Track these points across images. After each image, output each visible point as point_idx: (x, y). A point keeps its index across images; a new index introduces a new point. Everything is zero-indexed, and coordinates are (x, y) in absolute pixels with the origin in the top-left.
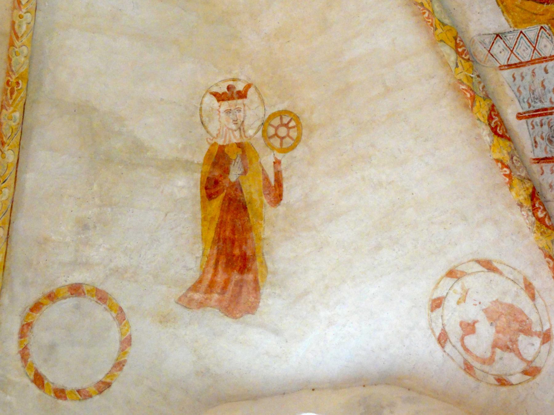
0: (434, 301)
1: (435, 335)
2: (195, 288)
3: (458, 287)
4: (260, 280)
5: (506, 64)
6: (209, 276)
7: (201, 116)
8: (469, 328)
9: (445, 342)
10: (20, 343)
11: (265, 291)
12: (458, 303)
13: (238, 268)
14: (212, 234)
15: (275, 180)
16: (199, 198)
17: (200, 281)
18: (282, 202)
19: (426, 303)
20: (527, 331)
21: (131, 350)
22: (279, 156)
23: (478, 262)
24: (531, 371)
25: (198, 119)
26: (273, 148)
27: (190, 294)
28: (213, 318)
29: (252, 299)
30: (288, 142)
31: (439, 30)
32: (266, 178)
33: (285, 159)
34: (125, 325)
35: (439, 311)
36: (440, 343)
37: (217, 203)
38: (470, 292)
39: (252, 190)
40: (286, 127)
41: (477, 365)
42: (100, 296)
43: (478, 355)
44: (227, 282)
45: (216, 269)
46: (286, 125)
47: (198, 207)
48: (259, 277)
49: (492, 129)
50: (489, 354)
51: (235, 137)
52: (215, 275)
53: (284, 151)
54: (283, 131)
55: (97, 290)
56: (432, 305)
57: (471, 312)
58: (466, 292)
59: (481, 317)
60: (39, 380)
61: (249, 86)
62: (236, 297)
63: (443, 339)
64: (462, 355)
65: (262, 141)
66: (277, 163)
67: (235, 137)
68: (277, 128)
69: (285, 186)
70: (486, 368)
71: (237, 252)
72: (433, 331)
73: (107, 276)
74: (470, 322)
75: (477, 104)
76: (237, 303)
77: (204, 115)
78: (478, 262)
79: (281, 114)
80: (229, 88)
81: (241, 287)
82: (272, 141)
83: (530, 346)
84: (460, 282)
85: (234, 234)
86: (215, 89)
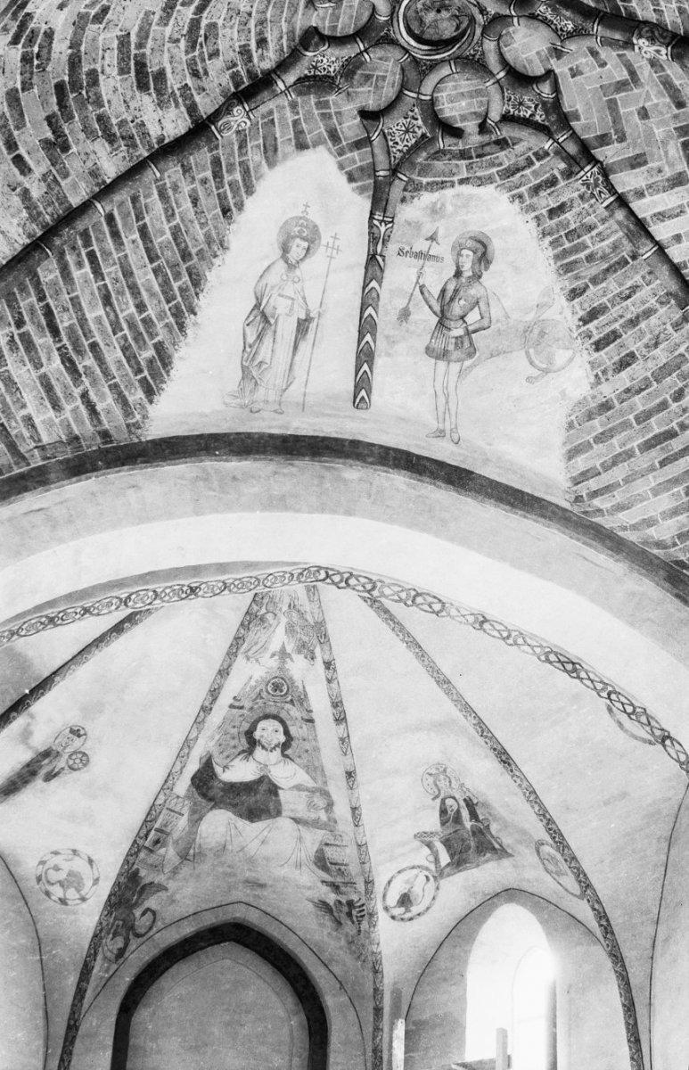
8: (57, 868)
24: (63, 901)
32: (53, 770)
37: (27, 769)
54: (78, 761)
57: (66, 867)
59: (66, 871)
61: (85, 734)
63: (42, 863)
66: (63, 769)
79: (84, 754)
80: (78, 730)
83: (72, 894)
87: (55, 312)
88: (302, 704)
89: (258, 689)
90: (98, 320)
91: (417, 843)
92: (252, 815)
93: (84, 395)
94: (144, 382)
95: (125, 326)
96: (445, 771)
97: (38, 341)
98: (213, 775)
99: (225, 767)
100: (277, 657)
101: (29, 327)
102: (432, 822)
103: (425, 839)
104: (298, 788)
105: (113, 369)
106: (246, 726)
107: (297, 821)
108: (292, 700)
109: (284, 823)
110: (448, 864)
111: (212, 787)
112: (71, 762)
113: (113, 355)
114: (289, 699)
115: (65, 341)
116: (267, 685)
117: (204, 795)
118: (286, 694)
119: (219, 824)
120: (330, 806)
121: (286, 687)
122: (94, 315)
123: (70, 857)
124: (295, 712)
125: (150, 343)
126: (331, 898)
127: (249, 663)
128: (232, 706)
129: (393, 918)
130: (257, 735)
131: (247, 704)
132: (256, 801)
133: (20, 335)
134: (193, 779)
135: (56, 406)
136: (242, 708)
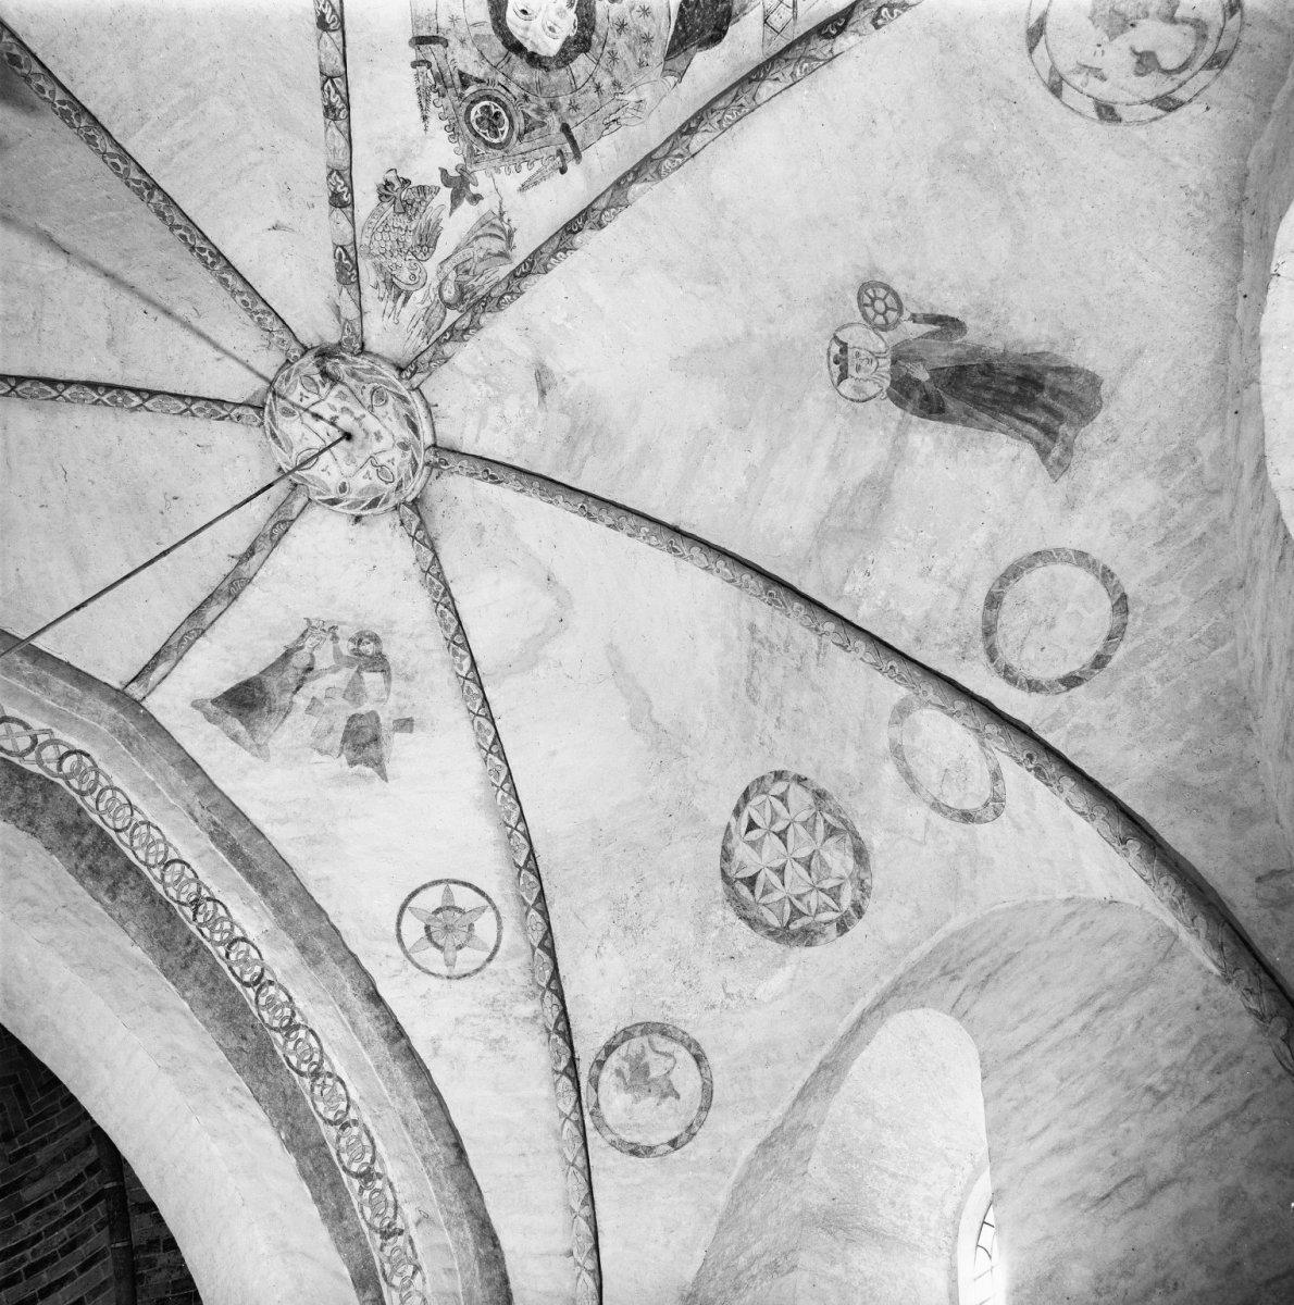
0: (1100, 115)
1: (1161, 117)
2: (1044, 453)
3: (1078, 80)
4: (1057, 365)
5: (791, 10)
6: (1034, 431)
7: (858, 401)
8: (1145, 62)
9: (1174, 101)
10: (1021, 687)
11: (1073, 359)
12: (1103, 79)
13: (1034, 391)
14: (985, 417)
15: (934, 324)
16: (940, 424)
17: (1037, 445)
18: (960, 319)
19: (1105, 130)
21: (1095, 555)
22: (907, 315)
23: (1031, 50)
25: (860, 406)
26: (898, 322)
27: (1050, 460)
28: (1092, 436)
29: (1081, 380)
30: (890, 300)
31: (742, 101)
32: (932, 334)
33: (910, 308)
34: (1058, 555)
35: (1120, 110)
36: (1175, 109)
37: (951, 405)
38: (1083, 61)
39: (944, 354)
40: (878, 300)
41: (1209, 49)
42: (1011, 575)
43: (1192, 47)
44: (1048, 409)
45: (1027, 420)
46: (873, 300)
47: (949, 426)
48: (1054, 365)
49: (838, 34)
50: (1187, 28)
51: (884, 366)
52: (1035, 424)
53: (900, 310)
54: (880, 306)
55: (1003, 576)
56: (1109, 120)
58: (1084, 68)
59: (1123, 42)
60: (1072, 681)
61: (835, 337)
62: (1074, 401)
63: (1167, 104)
64: (1196, 73)
65: (890, 332)
66: (914, 318)
67: (884, 366)
68: (877, 313)
69: (940, 313)
70: (1213, 33)
71: (1013, 389)
72: (1155, 119)
73: (993, 560)
74: (1135, 60)
75: (813, 53)
76: (1081, 401)
77: (858, 397)
78: (1031, 50)
79: (862, 305)
80: (836, 363)
81: (1060, 391)
82: (890, 321)
84: (1067, 77)
85: (991, 388)
86: (836, 379)
88: (439, 77)
89: (524, 147)
100: (473, 190)
106: (582, 64)
108: (465, 85)
112: (892, 315)
114: (471, 89)
116: (507, 142)
118: (474, 102)
121: (473, 117)
123: (1078, 80)
124: (465, 59)
127: (514, 224)
131: (553, 121)
134: (717, 36)
136: (566, 129)
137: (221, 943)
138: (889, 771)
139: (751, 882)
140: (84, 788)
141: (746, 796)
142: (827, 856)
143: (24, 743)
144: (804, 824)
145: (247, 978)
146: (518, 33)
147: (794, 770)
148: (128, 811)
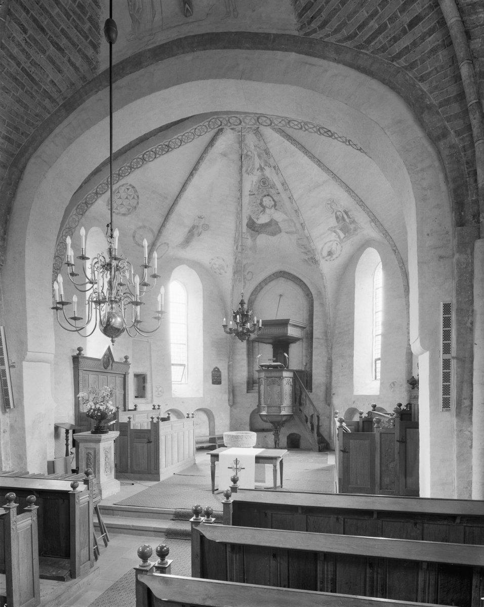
20: (223, 270)
24: (220, 274)
40: (206, 227)
63: (210, 263)
87: (37, 18)
90: (58, 14)
91: (330, 232)
92: (273, 234)
93: (69, 60)
94: (91, 43)
95: (71, 14)
96: (333, 200)
97: (38, 38)
98: (254, 223)
99: (258, 219)
101: (30, 32)
102: (333, 222)
103: (333, 230)
104: (284, 220)
105: (75, 40)
106: (259, 202)
107: (287, 233)
109: (283, 234)
110: (344, 237)
111: (255, 227)
113: (73, 33)
115: (50, 33)
117: (253, 230)
119: (263, 239)
120: (295, 226)
122: (55, 12)
125: (86, 19)
126: (306, 257)
128: (250, 195)
129: (326, 260)
130: (264, 203)
132: (271, 228)
133: (28, 37)
134: (247, 225)
135: (60, 71)
137: (156, 150)
138: (140, 224)
139: (118, 192)
140: (211, 123)
141: (133, 187)
142: (124, 208)
143: (231, 121)
144: (130, 203)
145: (145, 156)
146: (269, 197)
147: (139, 202)
148: (199, 134)
